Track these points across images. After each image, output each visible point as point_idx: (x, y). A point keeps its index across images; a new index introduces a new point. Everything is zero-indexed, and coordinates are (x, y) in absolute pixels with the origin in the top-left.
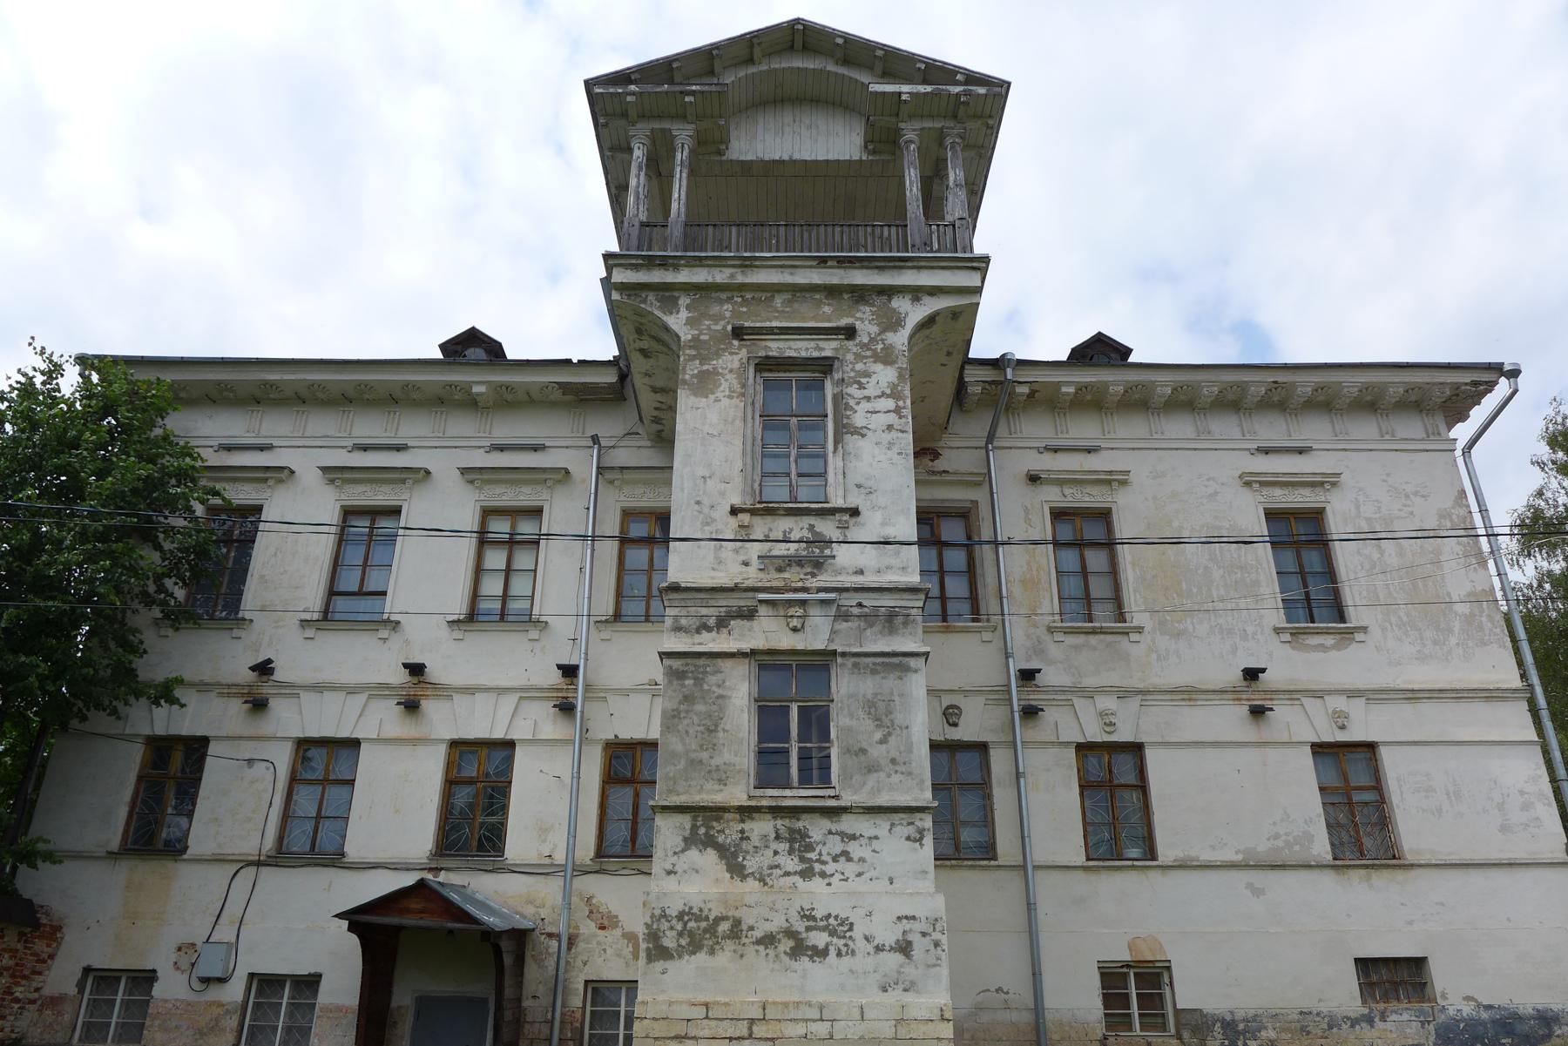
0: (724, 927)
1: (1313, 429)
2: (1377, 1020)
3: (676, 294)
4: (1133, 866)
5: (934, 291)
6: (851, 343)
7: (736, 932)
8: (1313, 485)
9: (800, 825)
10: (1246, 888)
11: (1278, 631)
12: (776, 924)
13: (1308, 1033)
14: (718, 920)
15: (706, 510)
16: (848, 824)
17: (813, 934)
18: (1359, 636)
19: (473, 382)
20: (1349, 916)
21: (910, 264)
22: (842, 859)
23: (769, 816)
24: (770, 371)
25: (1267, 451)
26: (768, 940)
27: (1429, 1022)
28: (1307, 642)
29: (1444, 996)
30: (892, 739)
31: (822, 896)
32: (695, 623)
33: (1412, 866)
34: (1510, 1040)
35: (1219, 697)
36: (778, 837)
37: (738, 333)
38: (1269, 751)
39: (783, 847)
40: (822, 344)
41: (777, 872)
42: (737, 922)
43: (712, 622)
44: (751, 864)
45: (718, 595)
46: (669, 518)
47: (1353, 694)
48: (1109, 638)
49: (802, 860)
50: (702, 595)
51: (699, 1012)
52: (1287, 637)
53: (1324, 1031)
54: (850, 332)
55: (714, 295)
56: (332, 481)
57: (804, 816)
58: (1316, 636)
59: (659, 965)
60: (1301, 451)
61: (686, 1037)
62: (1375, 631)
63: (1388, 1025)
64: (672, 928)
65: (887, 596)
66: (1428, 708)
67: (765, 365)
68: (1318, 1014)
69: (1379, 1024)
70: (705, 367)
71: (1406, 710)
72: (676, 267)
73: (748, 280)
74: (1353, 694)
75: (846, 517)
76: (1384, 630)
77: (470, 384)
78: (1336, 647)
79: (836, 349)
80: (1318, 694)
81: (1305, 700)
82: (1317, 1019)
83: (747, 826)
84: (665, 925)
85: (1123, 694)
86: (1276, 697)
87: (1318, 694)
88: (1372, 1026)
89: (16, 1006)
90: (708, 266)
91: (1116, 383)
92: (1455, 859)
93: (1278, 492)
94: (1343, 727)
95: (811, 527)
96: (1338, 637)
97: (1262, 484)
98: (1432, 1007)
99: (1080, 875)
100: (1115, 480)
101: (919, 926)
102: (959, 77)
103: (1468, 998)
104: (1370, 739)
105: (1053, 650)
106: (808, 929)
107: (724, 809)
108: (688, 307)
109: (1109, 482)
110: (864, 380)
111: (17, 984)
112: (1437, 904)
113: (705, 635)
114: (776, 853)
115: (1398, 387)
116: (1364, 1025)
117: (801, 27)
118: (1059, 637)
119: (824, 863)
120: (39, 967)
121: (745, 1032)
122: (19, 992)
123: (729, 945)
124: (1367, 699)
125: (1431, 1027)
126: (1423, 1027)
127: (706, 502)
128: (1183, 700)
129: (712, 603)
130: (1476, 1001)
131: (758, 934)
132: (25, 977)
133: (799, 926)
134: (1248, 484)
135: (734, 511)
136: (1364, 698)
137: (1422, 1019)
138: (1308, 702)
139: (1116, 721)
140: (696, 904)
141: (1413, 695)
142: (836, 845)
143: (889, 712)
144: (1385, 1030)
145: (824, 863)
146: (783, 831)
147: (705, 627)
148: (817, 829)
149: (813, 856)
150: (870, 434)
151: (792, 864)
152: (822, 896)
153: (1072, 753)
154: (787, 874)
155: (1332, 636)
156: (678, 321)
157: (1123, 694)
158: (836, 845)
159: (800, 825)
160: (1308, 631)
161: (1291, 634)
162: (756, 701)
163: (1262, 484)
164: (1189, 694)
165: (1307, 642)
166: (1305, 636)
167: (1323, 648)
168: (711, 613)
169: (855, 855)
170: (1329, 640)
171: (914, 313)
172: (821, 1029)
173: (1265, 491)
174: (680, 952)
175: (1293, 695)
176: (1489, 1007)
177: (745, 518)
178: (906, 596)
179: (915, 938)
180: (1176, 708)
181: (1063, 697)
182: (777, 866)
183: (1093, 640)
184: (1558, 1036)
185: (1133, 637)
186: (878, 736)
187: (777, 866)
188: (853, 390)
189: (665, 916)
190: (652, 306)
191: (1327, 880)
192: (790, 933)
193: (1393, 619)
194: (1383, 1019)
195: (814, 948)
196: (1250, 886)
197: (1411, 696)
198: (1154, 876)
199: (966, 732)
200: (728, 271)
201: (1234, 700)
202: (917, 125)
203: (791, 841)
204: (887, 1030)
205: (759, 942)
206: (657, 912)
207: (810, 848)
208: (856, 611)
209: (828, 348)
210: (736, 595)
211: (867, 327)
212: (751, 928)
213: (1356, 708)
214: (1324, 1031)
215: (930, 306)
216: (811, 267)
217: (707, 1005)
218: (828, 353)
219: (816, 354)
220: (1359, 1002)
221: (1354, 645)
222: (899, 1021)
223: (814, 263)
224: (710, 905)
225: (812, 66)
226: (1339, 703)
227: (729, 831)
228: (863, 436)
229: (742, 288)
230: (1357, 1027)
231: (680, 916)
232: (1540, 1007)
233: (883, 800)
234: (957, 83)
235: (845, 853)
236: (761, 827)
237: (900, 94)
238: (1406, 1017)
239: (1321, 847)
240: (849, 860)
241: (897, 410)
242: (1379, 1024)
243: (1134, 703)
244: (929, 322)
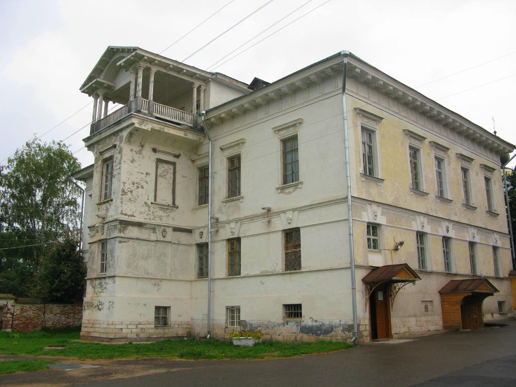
0: (91, 304)
2: (285, 324)
4: (234, 277)
5: (128, 127)
6: (115, 149)
8: (294, 125)
10: (260, 282)
11: (277, 189)
12: (96, 304)
13: (268, 328)
14: (91, 303)
18: (300, 186)
20: (284, 290)
21: (121, 121)
23: (98, 280)
24: (107, 162)
27: (299, 325)
28: (286, 192)
29: (304, 317)
30: (113, 259)
33: (302, 272)
34: (320, 332)
35: (259, 218)
41: (98, 292)
46: (240, 157)
47: (294, 210)
48: (236, 202)
51: (87, 322)
52: (279, 191)
53: (272, 327)
54: (115, 146)
58: (288, 189)
61: (92, 327)
63: (288, 326)
65: (114, 222)
68: (271, 322)
69: (286, 326)
71: (309, 213)
75: (110, 202)
79: (113, 152)
80: (284, 212)
82: (271, 324)
83: (96, 282)
85: (237, 221)
86: (274, 215)
87: (284, 212)
88: (284, 326)
89: (77, 320)
90: (96, 136)
91: (234, 108)
92: (316, 269)
93: (283, 132)
94: (289, 223)
96: (294, 187)
98: (300, 321)
99: (224, 281)
100: (240, 143)
103: (311, 318)
105: (224, 210)
106: (100, 304)
107: (92, 279)
109: (238, 144)
111: (75, 315)
112: (308, 285)
115: (313, 76)
116: (282, 326)
117: (109, 49)
118: (225, 204)
119: (103, 290)
120: (80, 312)
121: (92, 326)
122: (76, 317)
123: (91, 308)
124: (299, 211)
125: (299, 327)
126: (297, 327)
128: (250, 220)
130: (313, 319)
131: (94, 306)
132: (77, 314)
135: (98, 205)
136: (298, 211)
137: (297, 324)
138: (282, 215)
139: (234, 231)
143: (113, 253)
144: (287, 327)
148: (103, 281)
149: (102, 288)
150: (115, 176)
151: (100, 291)
153: (225, 243)
154: (99, 293)
155: (293, 188)
157: (237, 221)
160: (285, 187)
161: (281, 189)
162: (101, 252)
163: (279, 130)
164: (252, 218)
165: (286, 192)
166: (285, 189)
167: (290, 193)
169: (107, 288)
171: (125, 134)
172: (99, 325)
175: (278, 213)
176: (316, 321)
177: (99, 206)
178: (116, 222)
180: (249, 224)
181: (223, 225)
182: (98, 291)
183: (233, 203)
184: (334, 331)
185: (241, 200)
186: (111, 259)
191: (280, 278)
192: (98, 306)
194: (287, 324)
196: (261, 282)
197: (311, 207)
198: (239, 280)
199: (203, 240)
201: (263, 218)
202: (132, 68)
204: (105, 326)
208: (111, 227)
211: (118, 143)
214: (272, 327)
215: (129, 130)
220: (282, 319)
221: (298, 190)
222: (108, 324)
223: (108, 129)
228: (115, 177)
229: (102, 140)
230: (280, 326)
232: (330, 321)
234: (132, 52)
235: (106, 287)
236: (97, 282)
238: (293, 323)
242: (286, 326)
243: (239, 224)
244: (131, 134)
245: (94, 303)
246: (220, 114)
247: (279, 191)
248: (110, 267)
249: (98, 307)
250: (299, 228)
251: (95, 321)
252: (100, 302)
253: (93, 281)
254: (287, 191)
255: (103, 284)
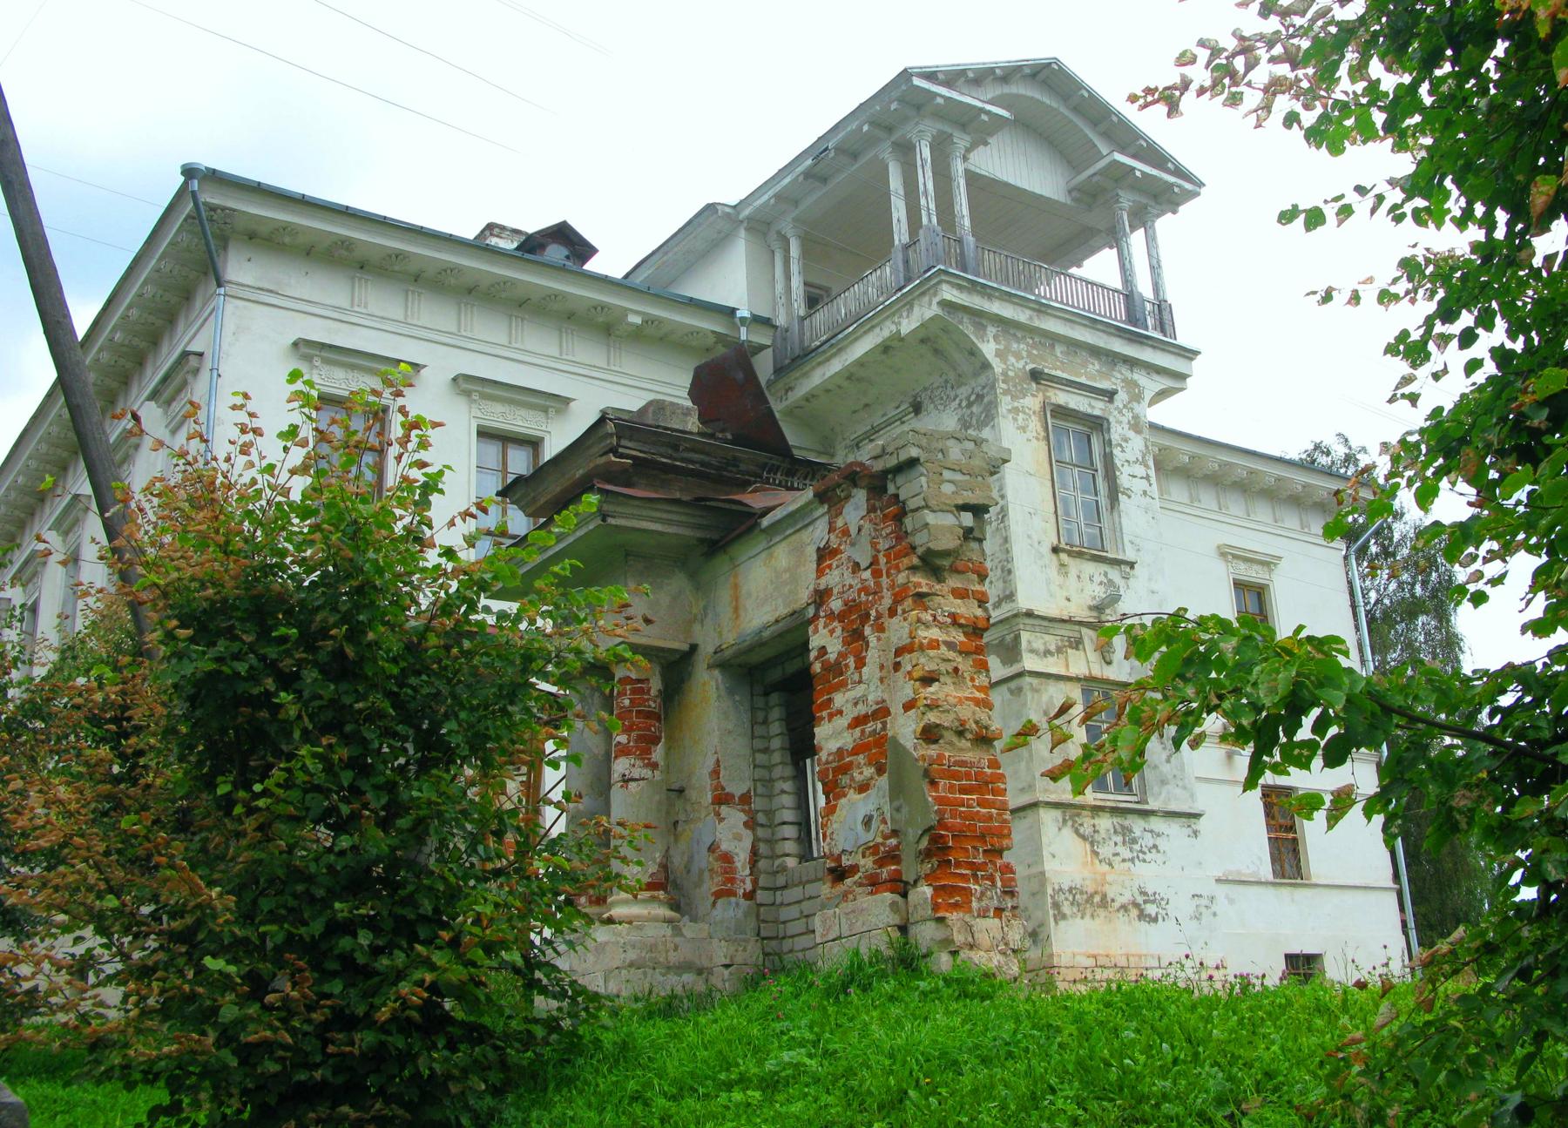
0: (1097, 899)
3: (984, 322)
7: (1105, 903)
9: (1126, 823)
14: (1092, 896)
15: (1036, 545)
16: (1156, 824)
17: (1148, 906)
19: (631, 310)
22: (1154, 851)
23: (1108, 815)
26: (1124, 907)
31: (1148, 875)
32: (1042, 648)
36: (1115, 832)
37: (1036, 376)
39: (1119, 839)
40: (1094, 402)
41: (1118, 859)
42: (1104, 896)
43: (1053, 648)
44: (1105, 851)
45: (1056, 625)
49: (1131, 850)
50: (1045, 623)
51: (1090, 962)
55: (1012, 331)
56: (467, 394)
57: (1129, 816)
59: (1062, 923)
64: (1067, 899)
67: (1061, 412)
70: (1016, 404)
72: (990, 297)
73: (1043, 326)
77: (626, 311)
83: (1096, 821)
84: (1062, 897)
93: (1242, 566)
95: (1106, 574)
97: (1235, 557)
101: (1204, 902)
102: (1170, 165)
106: (1145, 902)
108: (995, 338)
110: (1124, 444)
113: (1050, 659)
114: (1116, 844)
123: (1101, 912)
127: (1035, 538)
129: (1051, 631)
131: (1117, 905)
133: (1140, 900)
134: (1223, 555)
140: (1078, 883)
142: (1148, 840)
145: (1144, 853)
146: (1117, 827)
147: (1047, 653)
148: (1137, 825)
149: (1137, 847)
152: (1148, 875)
154: (1124, 860)
156: (989, 349)
158: (1148, 840)
159: (1126, 823)
168: (1052, 642)
174: (1074, 915)
179: (1203, 910)
182: (1117, 854)
187: (1117, 854)
188: (1117, 451)
189: (1061, 889)
190: (968, 328)
191: (1271, 891)
192: (1136, 905)
195: (1150, 916)
200: (1028, 312)
203: (1124, 835)
205: (1118, 910)
206: (1057, 887)
207: (1134, 841)
209: (1097, 407)
210: (1068, 626)
212: (1113, 900)
216: (1085, 325)
217: (1095, 957)
218: (1097, 412)
219: (1089, 411)
224: (1088, 882)
225: (1048, 102)
227: (1087, 823)
231: (1070, 890)
233: (1173, 807)
235: (1155, 846)
236: (1105, 823)
237: (1134, 169)
239: (1266, 870)
240: (1158, 851)
241: (1147, 478)
245: (1110, 895)
248: (1163, 782)
249: (1141, 911)
251: (1131, 959)
252: (1145, 894)
253: (1078, 815)
255: (1137, 832)
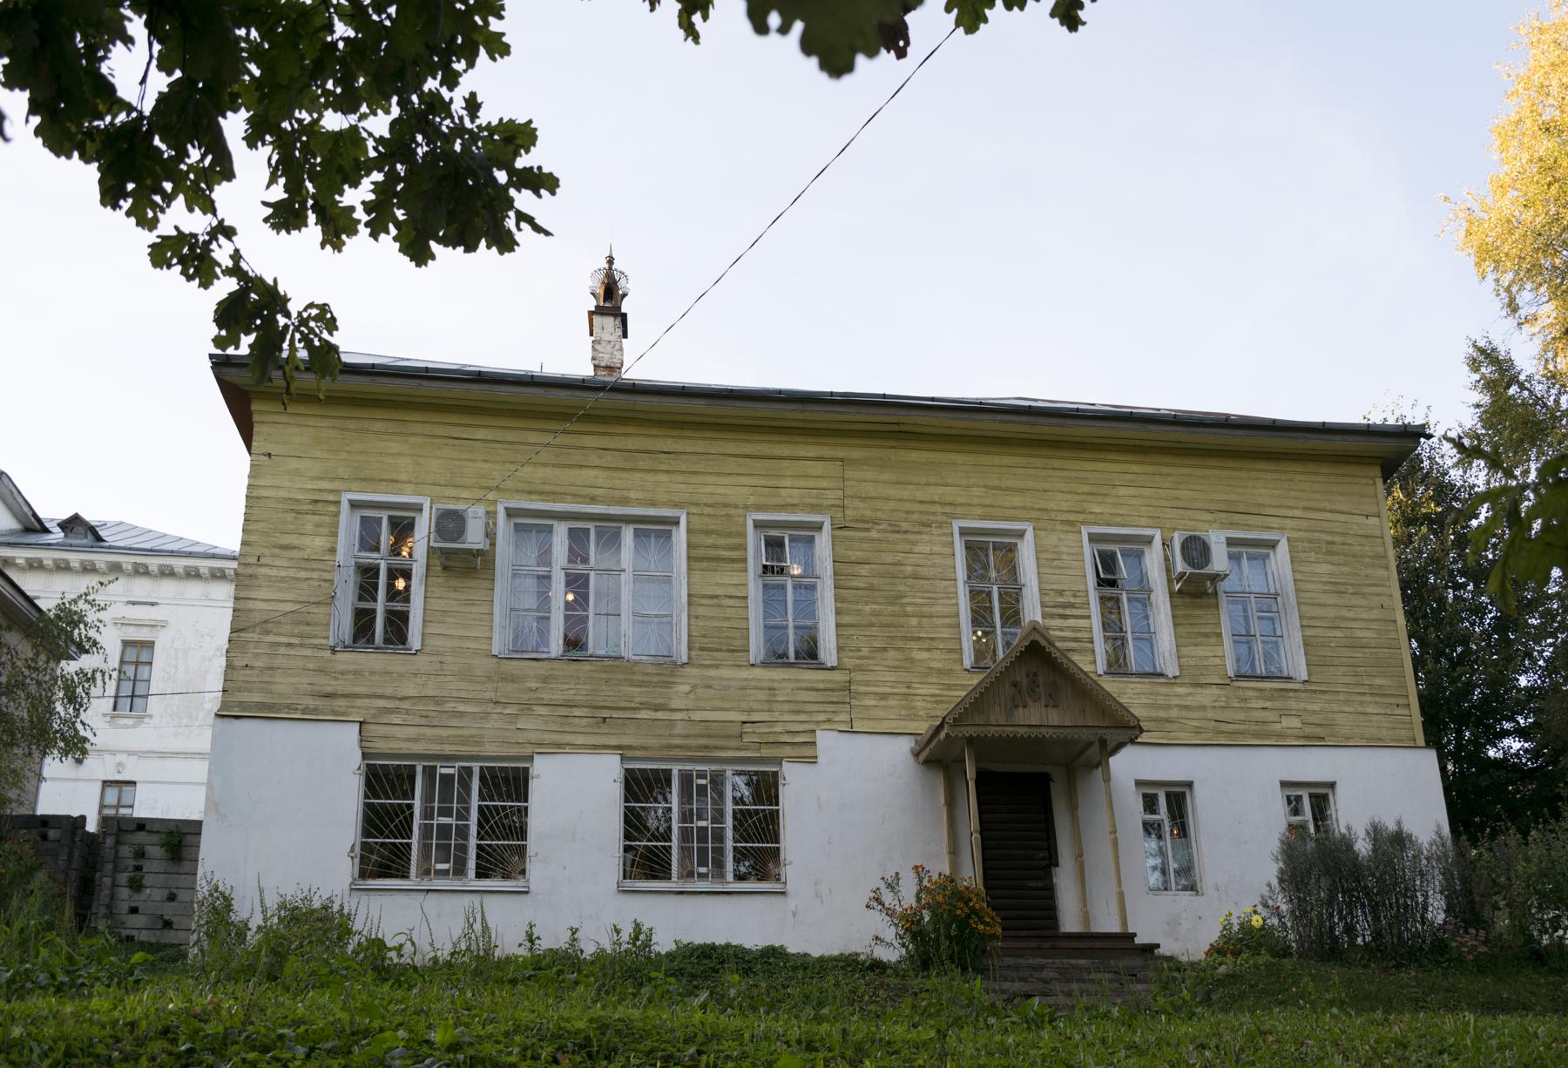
1: (166, 589)
18: (146, 720)
25: (134, 603)
38: (80, 784)
47: (131, 753)
52: (108, 719)
60: (153, 604)
62: (155, 721)
66: (170, 763)
71: (157, 763)
74: (131, 753)
76: (162, 717)
78: (133, 727)
80: (113, 753)
81: (106, 756)
87: (113, 753)
91: (47, 559)
93: (131, 629)
94: (119, 772)
104: (132, 779)
138: (107, 757)
141: (162, 755)
167: (126, 727)
170: (130, 722)
173: (124, 628)
193: (169, 711)
213: (131, 762)
221: (143, 726)
226: (121, 758)
246: (14, 558)
247: (108, 719)
250: (134, 783)
254: (122, 721)
